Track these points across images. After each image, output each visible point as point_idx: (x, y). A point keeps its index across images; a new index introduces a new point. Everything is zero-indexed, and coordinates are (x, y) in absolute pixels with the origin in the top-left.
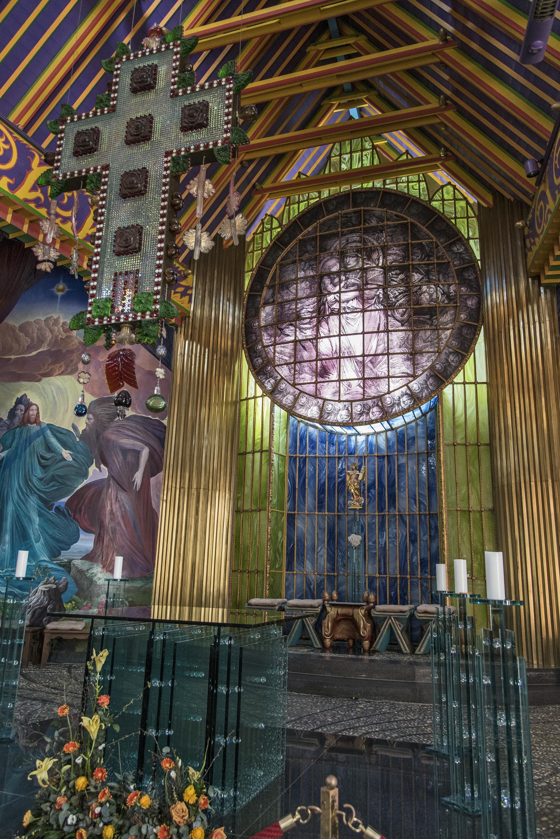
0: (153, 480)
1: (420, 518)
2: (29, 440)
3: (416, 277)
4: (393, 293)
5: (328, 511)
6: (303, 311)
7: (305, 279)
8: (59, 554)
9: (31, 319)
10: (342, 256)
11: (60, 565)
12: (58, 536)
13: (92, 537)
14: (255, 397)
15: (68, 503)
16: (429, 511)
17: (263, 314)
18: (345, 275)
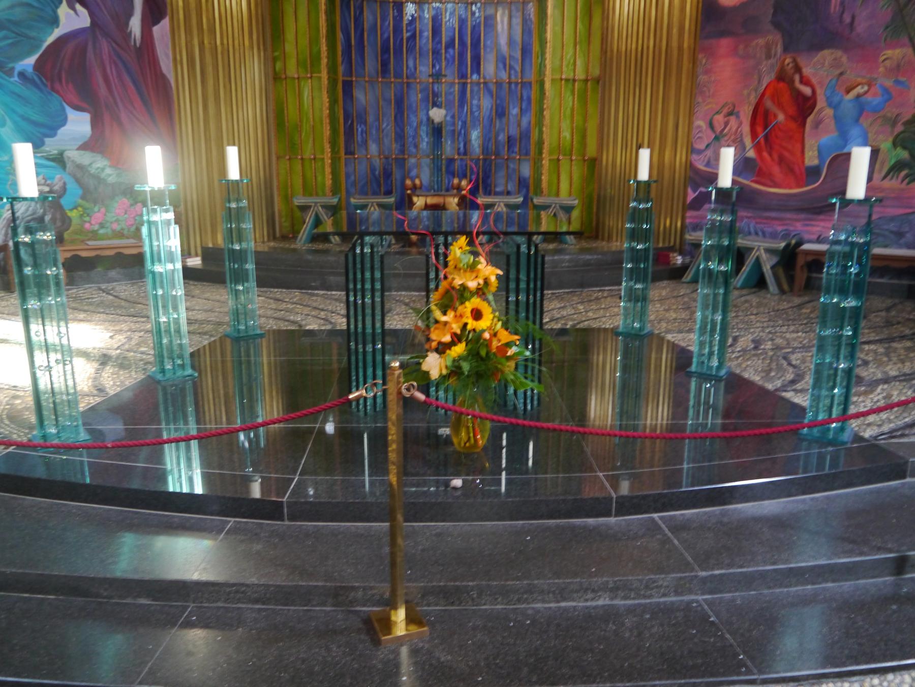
0: (156, 29)
1: (510, 87)
5: (395, 77)
8: (43, 144)
11: (48, 159)
12: (35, 117)
13: (86, 117)
15: (39, 66)
16: (522, 78)
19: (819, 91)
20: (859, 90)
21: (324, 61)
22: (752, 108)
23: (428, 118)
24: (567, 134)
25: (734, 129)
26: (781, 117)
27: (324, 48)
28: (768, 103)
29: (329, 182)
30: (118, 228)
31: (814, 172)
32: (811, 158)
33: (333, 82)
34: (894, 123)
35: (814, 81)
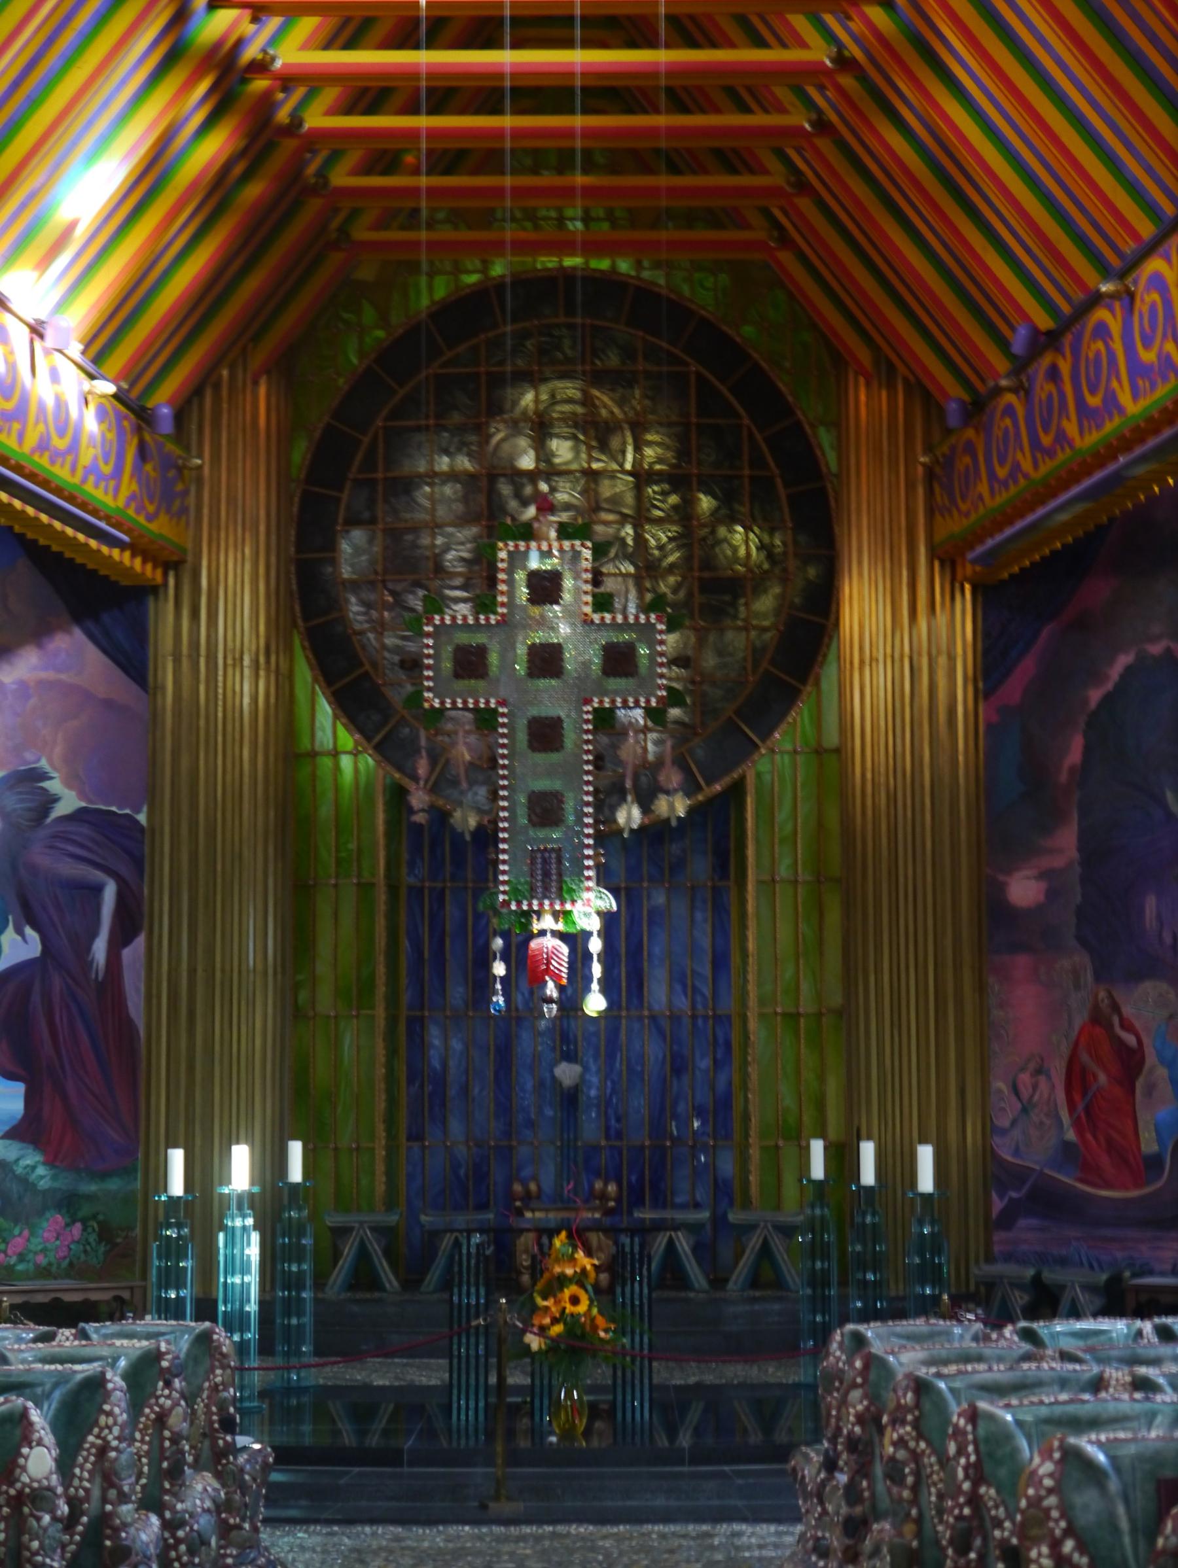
0: (127, 953)
1: (694, 1024)
3: (705, 503)
4: (656, 537)
6: (449, 556)
7: (452, 476)
10: (541, 429)
13: (19, 1088)
14: (335, 754)
16: (714, 1010)
17: (345, 547)
18: (548, 481)
19: (1145, 1040)
21: (381, 990)
22: (1064, 1064)
23: (553, 1077)
24: (789, 1101)
25: (1046, 1096)
26: (1102, 1078)
27: (381, 970)
28: (1085, 1057)
29: (380, 1188)
30: (43, 1261)
31: (1155, 1163)
32: (1149, 1144)
33: (392, 1021)
35: (1138, 1025)
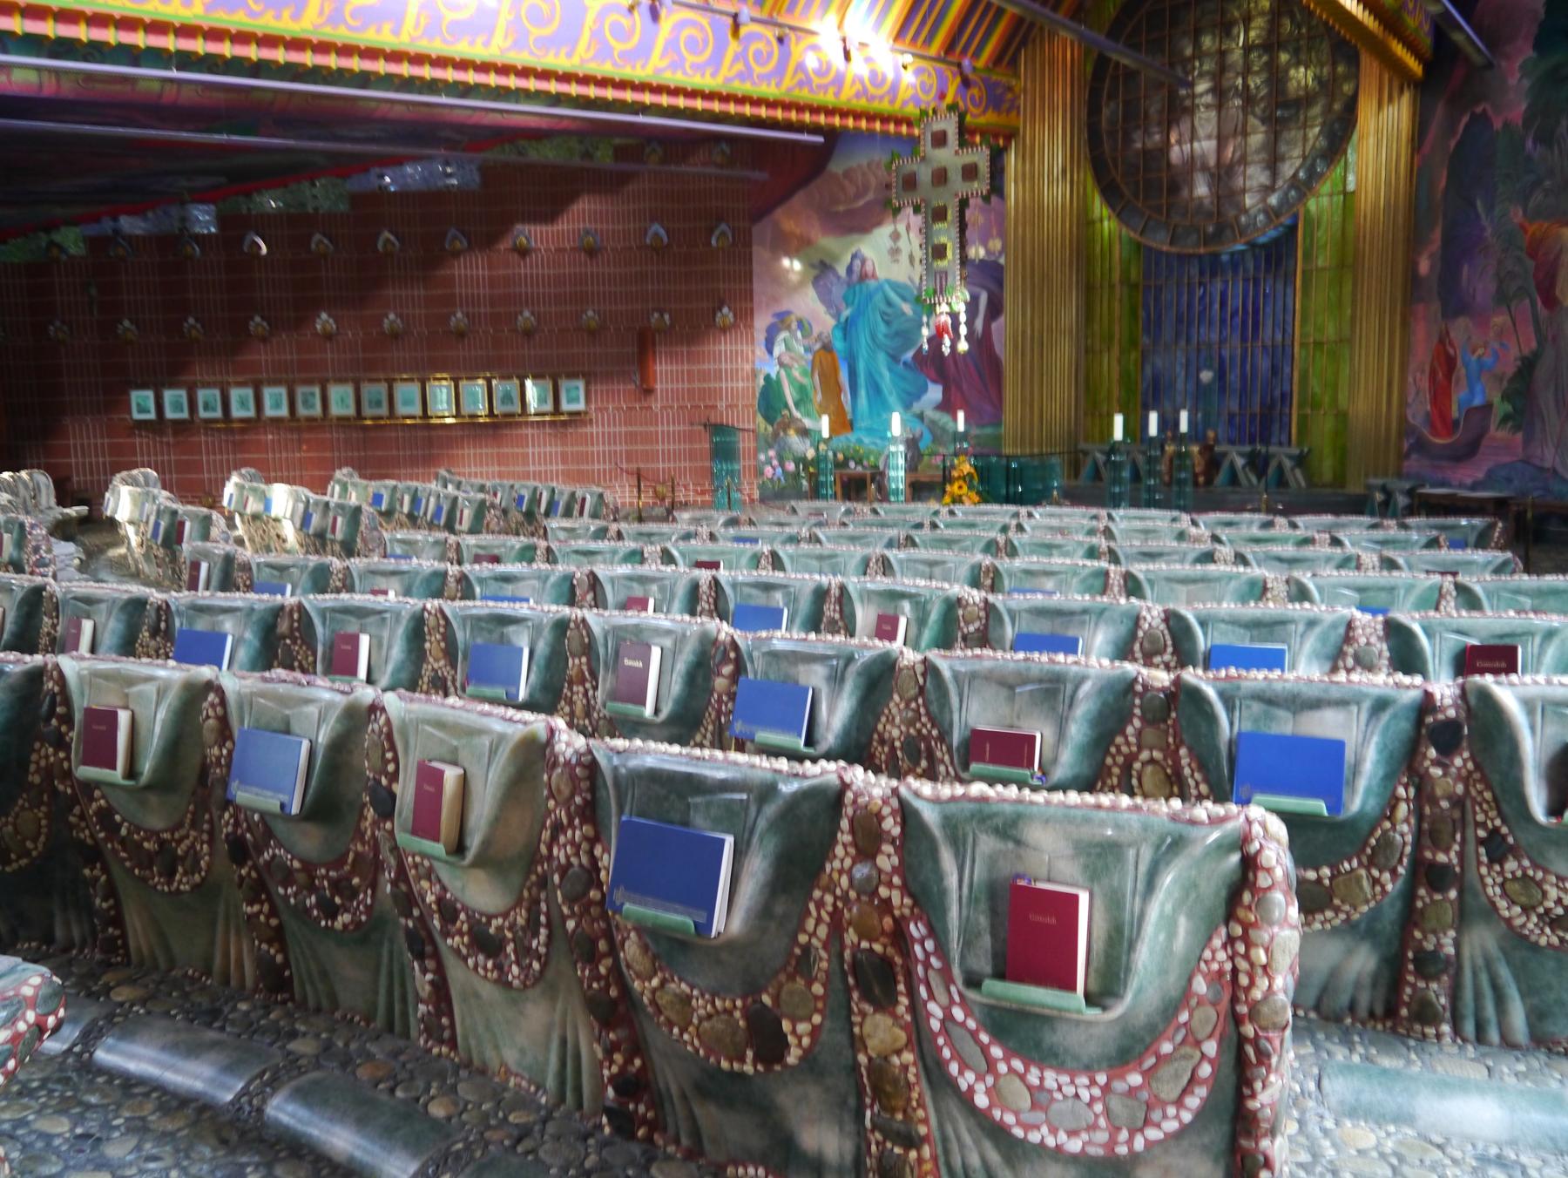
0: (994, 326)
2: (870, 296)
9: (853, 163)
14: (1101, 221)
20: (1480, 351)
34: (1501, 380)
